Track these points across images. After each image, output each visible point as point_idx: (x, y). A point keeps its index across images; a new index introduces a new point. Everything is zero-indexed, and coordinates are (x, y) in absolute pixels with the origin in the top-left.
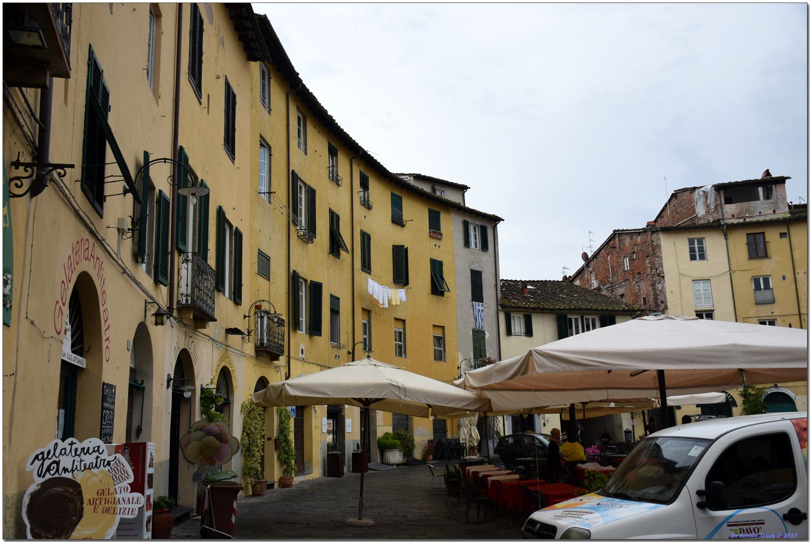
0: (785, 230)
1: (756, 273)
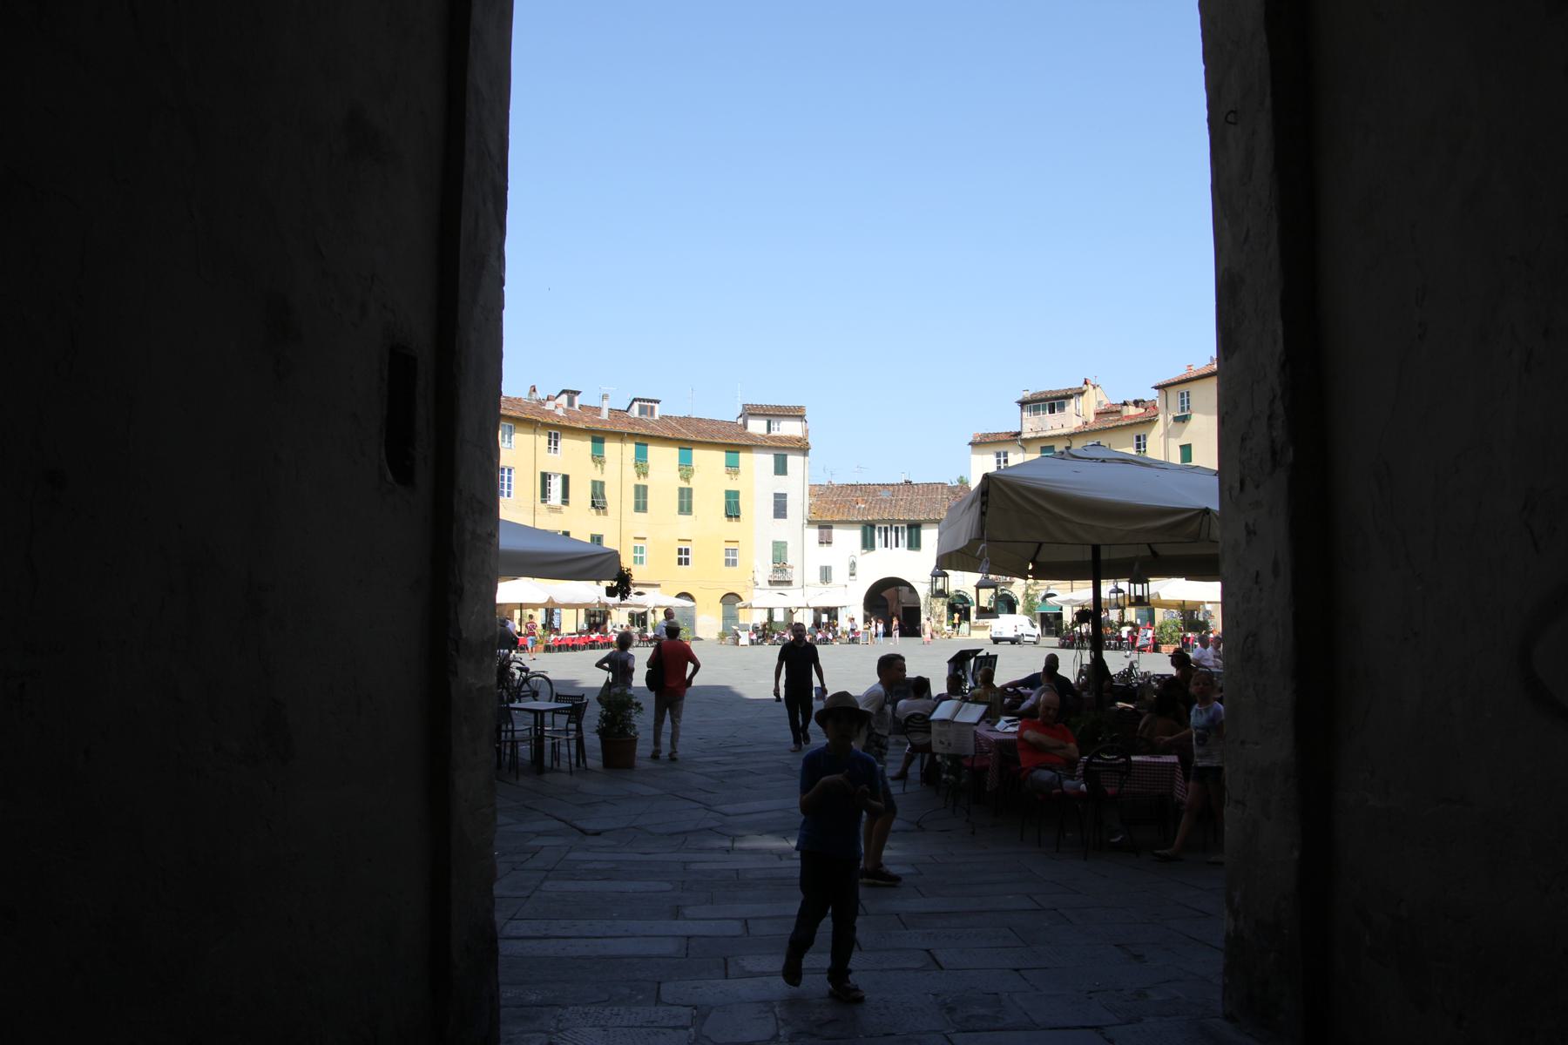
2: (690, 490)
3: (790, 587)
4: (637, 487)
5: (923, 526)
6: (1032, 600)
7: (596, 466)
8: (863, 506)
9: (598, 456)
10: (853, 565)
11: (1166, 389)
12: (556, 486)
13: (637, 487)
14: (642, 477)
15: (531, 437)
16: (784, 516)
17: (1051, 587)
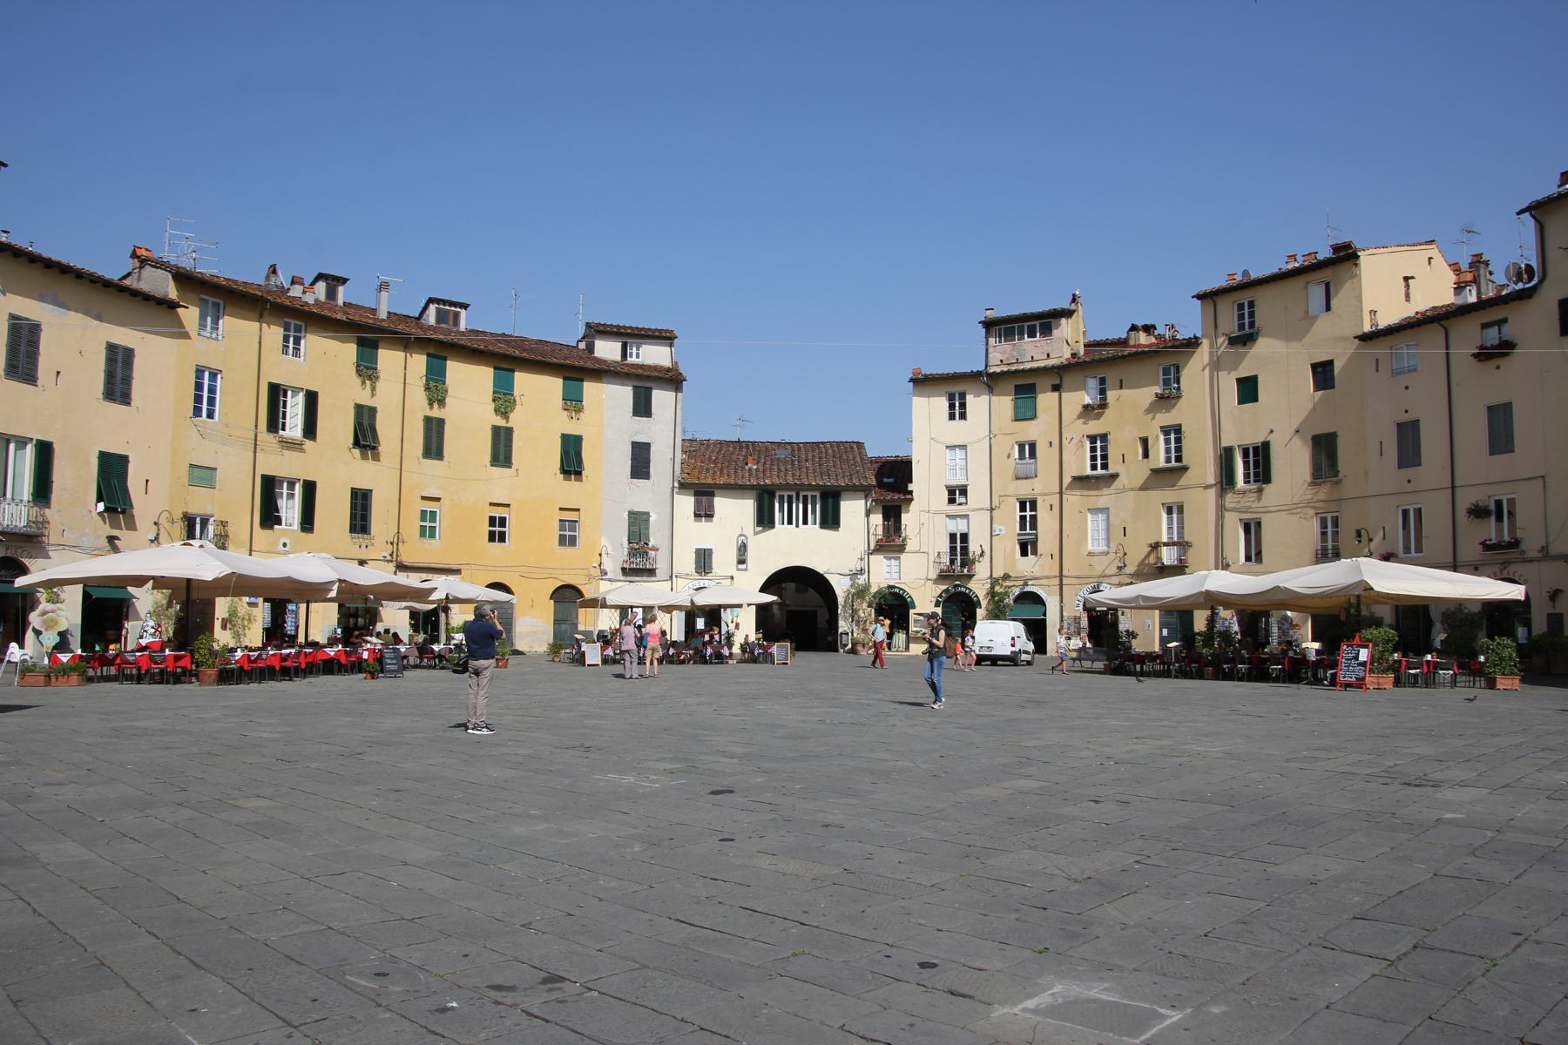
0: (1057, 382)
1: (1022, 439)
2: (509, 431)
3: (653, 579)
4: (428, 421)
5: (844, 495)
6: (1002, 600)
7: (363, 383)
8: (755, 467)
9: (367, 368)
10: (743, 548)
11: (1215, 298)
12: (295, 409)
14: (436, 406)
15: (253, 326)
16: (646, 476)
17: (1030, 583)
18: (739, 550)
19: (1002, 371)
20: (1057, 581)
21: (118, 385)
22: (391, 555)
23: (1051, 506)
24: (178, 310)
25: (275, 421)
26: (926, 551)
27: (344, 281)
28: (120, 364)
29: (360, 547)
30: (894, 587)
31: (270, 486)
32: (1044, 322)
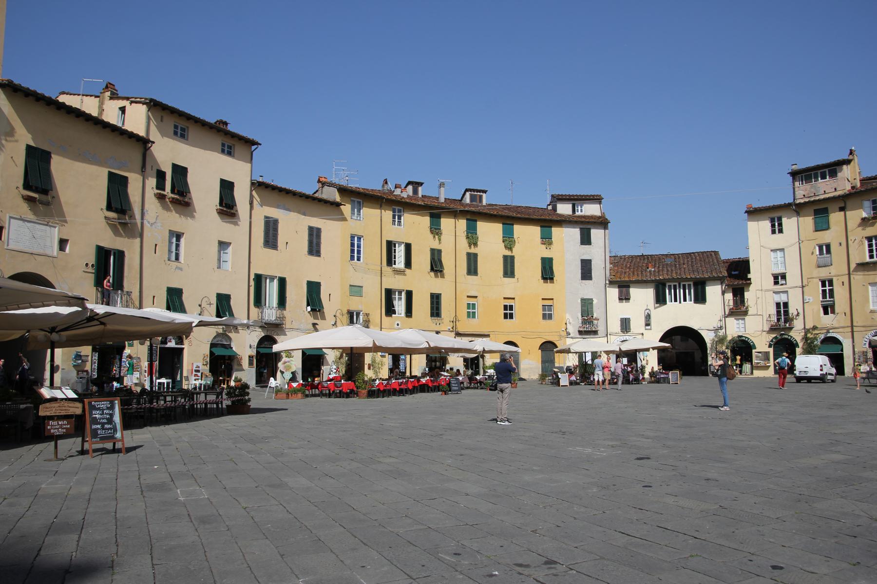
0: (842, 205)
1: (820, 242)
2: (512, 258)
3: (597, 336)
4: (469, 255)
5: (708, 283)
7: (434, 237)
8: (653, 270)
10: (648, 317)
12: (400, 253)
13: (469, 255)
14: (472, 246)
15: (377, 212)
16: (590, 278)
17: (831, 331)
18: (646, 318)
19: (805, 202)
20: (849, 329)
21: (314, 249)
22: (453, 328)
23: (843, 282)
24: (341, 207)
25: (390, 261)
26: (761, 314)
27: (421, 184)
28: (315, 237)
29: (436, 324)
30: (742, 336)
31: (389, 294)
32: (832, 169)
